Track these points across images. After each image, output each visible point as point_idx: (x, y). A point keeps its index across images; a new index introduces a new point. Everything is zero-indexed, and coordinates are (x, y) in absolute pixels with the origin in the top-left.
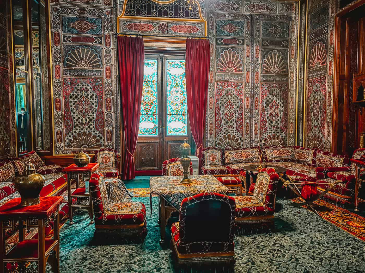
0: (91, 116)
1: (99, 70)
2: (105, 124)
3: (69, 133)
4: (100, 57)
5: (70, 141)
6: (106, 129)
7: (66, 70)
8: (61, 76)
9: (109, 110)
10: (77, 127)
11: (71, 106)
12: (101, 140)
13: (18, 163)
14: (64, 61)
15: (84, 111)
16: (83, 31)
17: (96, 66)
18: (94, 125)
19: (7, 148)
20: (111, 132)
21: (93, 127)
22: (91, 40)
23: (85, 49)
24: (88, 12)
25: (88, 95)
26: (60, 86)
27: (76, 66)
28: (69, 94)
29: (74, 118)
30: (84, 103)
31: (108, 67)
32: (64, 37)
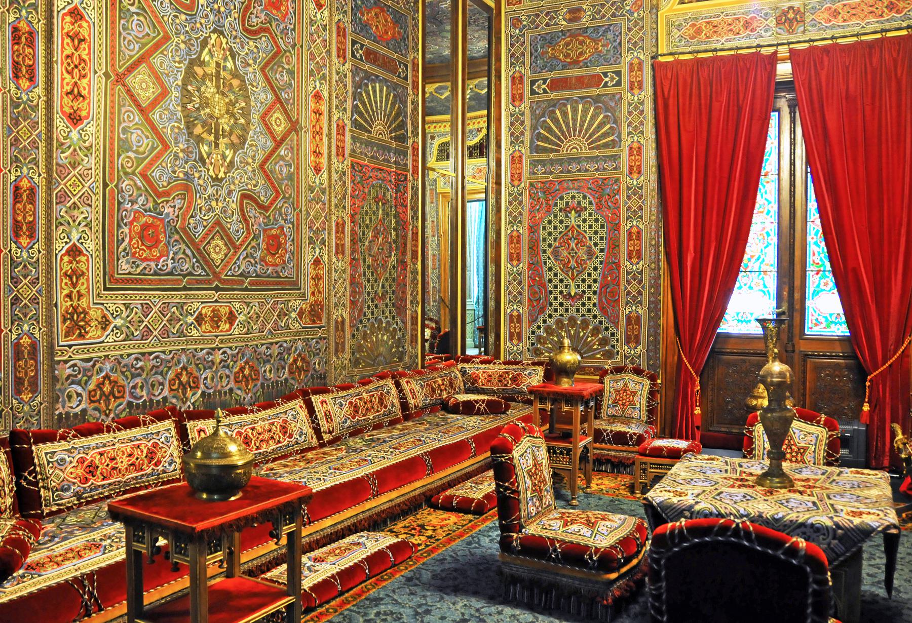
0: (589, 275)
1: (612, 156)
2: (623, 299)
3: (537, 318)
4: (615, 122)
5: (539, 338)
6: (625, 311)
7: (534, 163)
8: (523, 179)
9: (635, 261)
10: (556, 304)
11: (544, 252)
12: (614, 342)
13: (407, 382)
14: (532, 142)
15: (573, 263)
16: (575, 63)
17: (606, 146)
18: (595, 299)
19: (398, 347)
20: (638, 318)
21: (594, 305)
22: (596, 80)
23: (580, 106)
24: (589, 13)
25: (584, 221)
26: (520, 203)
27: (558, 151)
28: (541, 219)
29: (550, 281)
30: (573, 245)
31: (635, 145)
32: (533, 83)
